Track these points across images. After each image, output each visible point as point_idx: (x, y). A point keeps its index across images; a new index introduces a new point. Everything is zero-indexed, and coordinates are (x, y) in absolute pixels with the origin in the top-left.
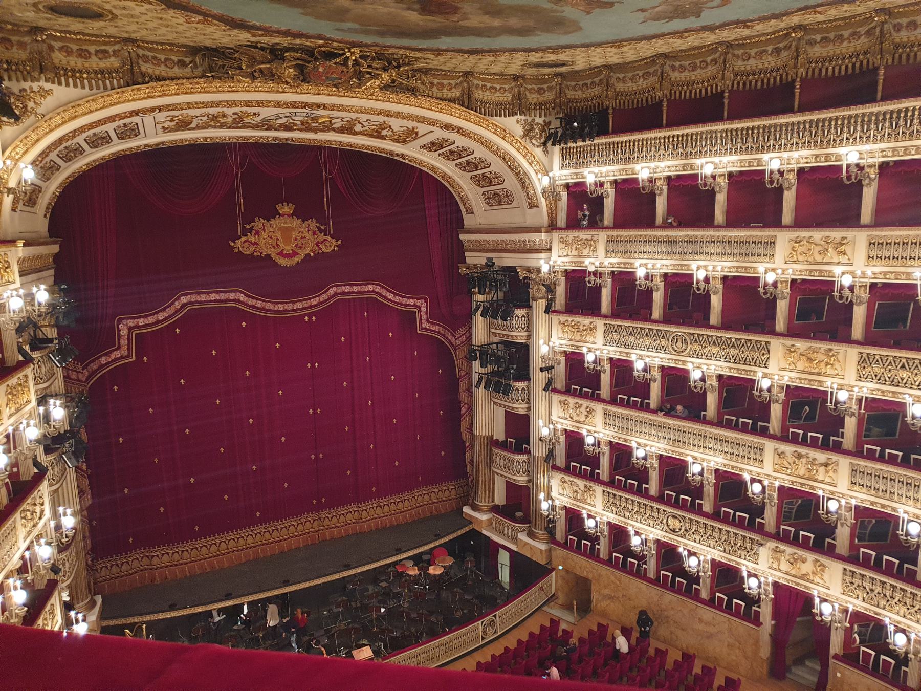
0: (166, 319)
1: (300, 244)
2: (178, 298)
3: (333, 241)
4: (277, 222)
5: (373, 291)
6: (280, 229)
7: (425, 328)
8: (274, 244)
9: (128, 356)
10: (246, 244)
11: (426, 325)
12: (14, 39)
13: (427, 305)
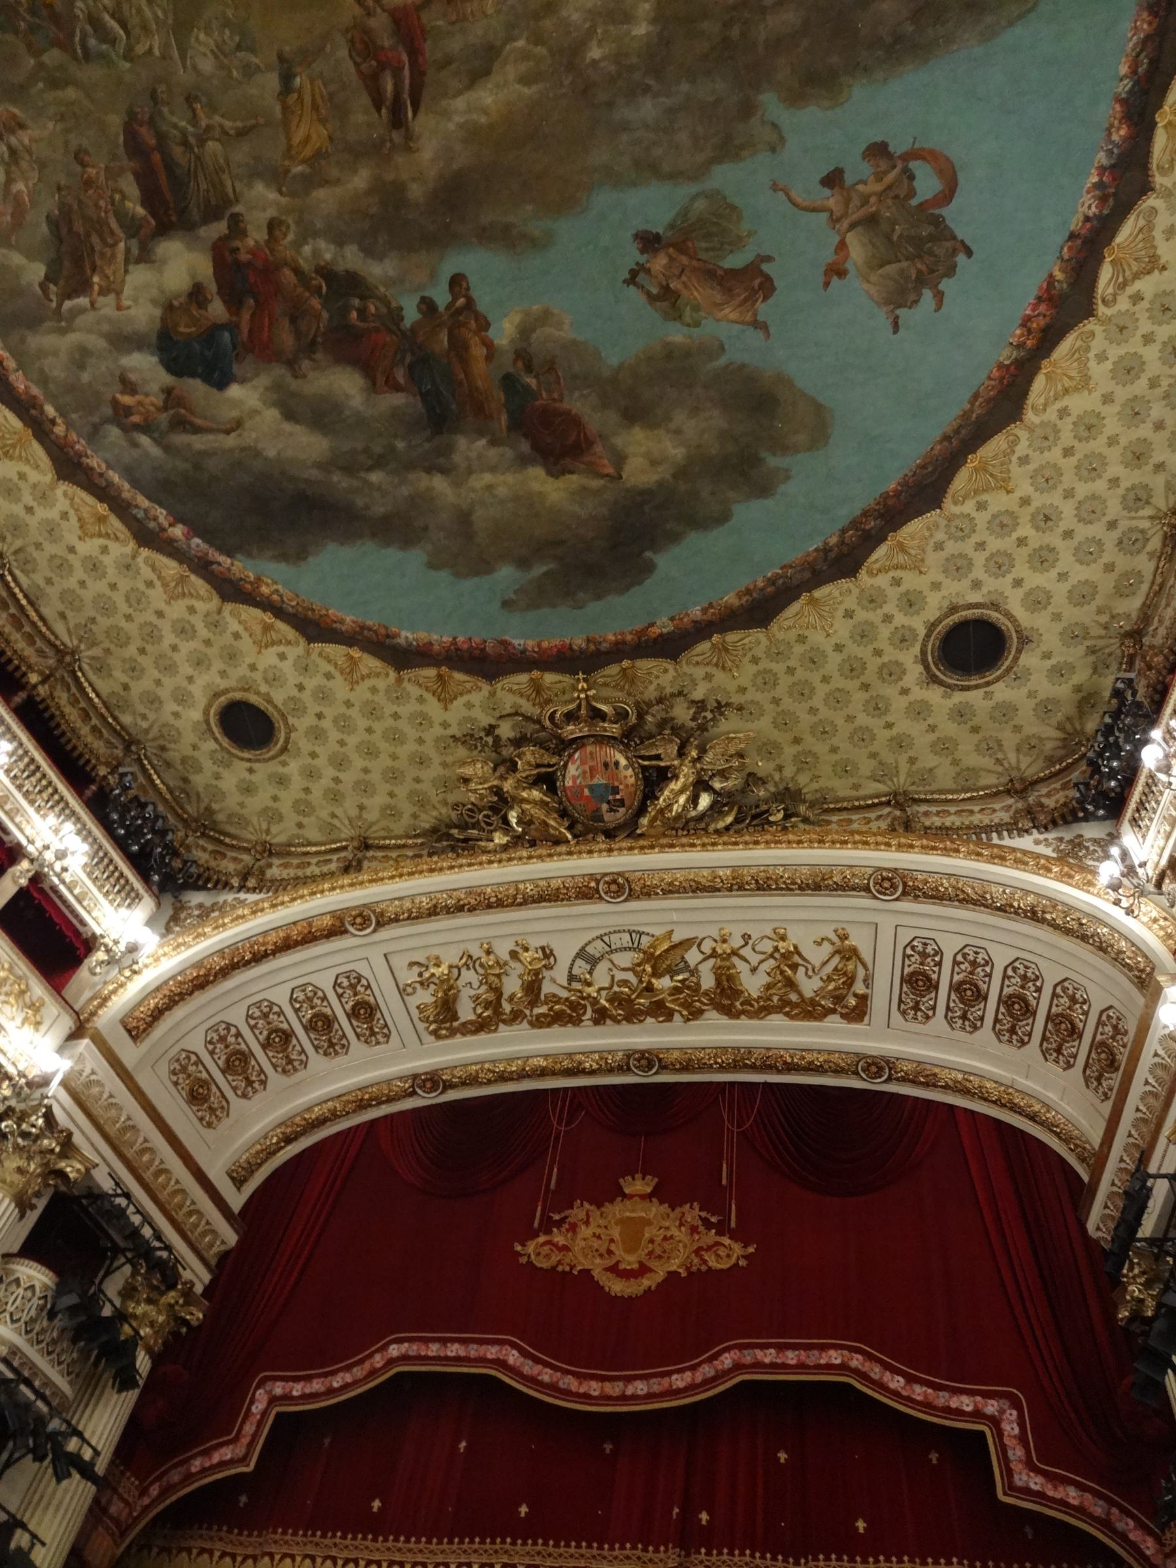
0: (345, 1387)
1: (658, 1251)
2: (384, 1348)
3: (738, 1249)
4: (617, 1210)
5: (843, 1367)
6: (622, 1222)
7: (1026, 1491)
8: (603, 1250)
9: (243, 1460)
10: (546, 1248)
11: (1023, 1478)
12: (230, 854)
13: (1021, 1416)
